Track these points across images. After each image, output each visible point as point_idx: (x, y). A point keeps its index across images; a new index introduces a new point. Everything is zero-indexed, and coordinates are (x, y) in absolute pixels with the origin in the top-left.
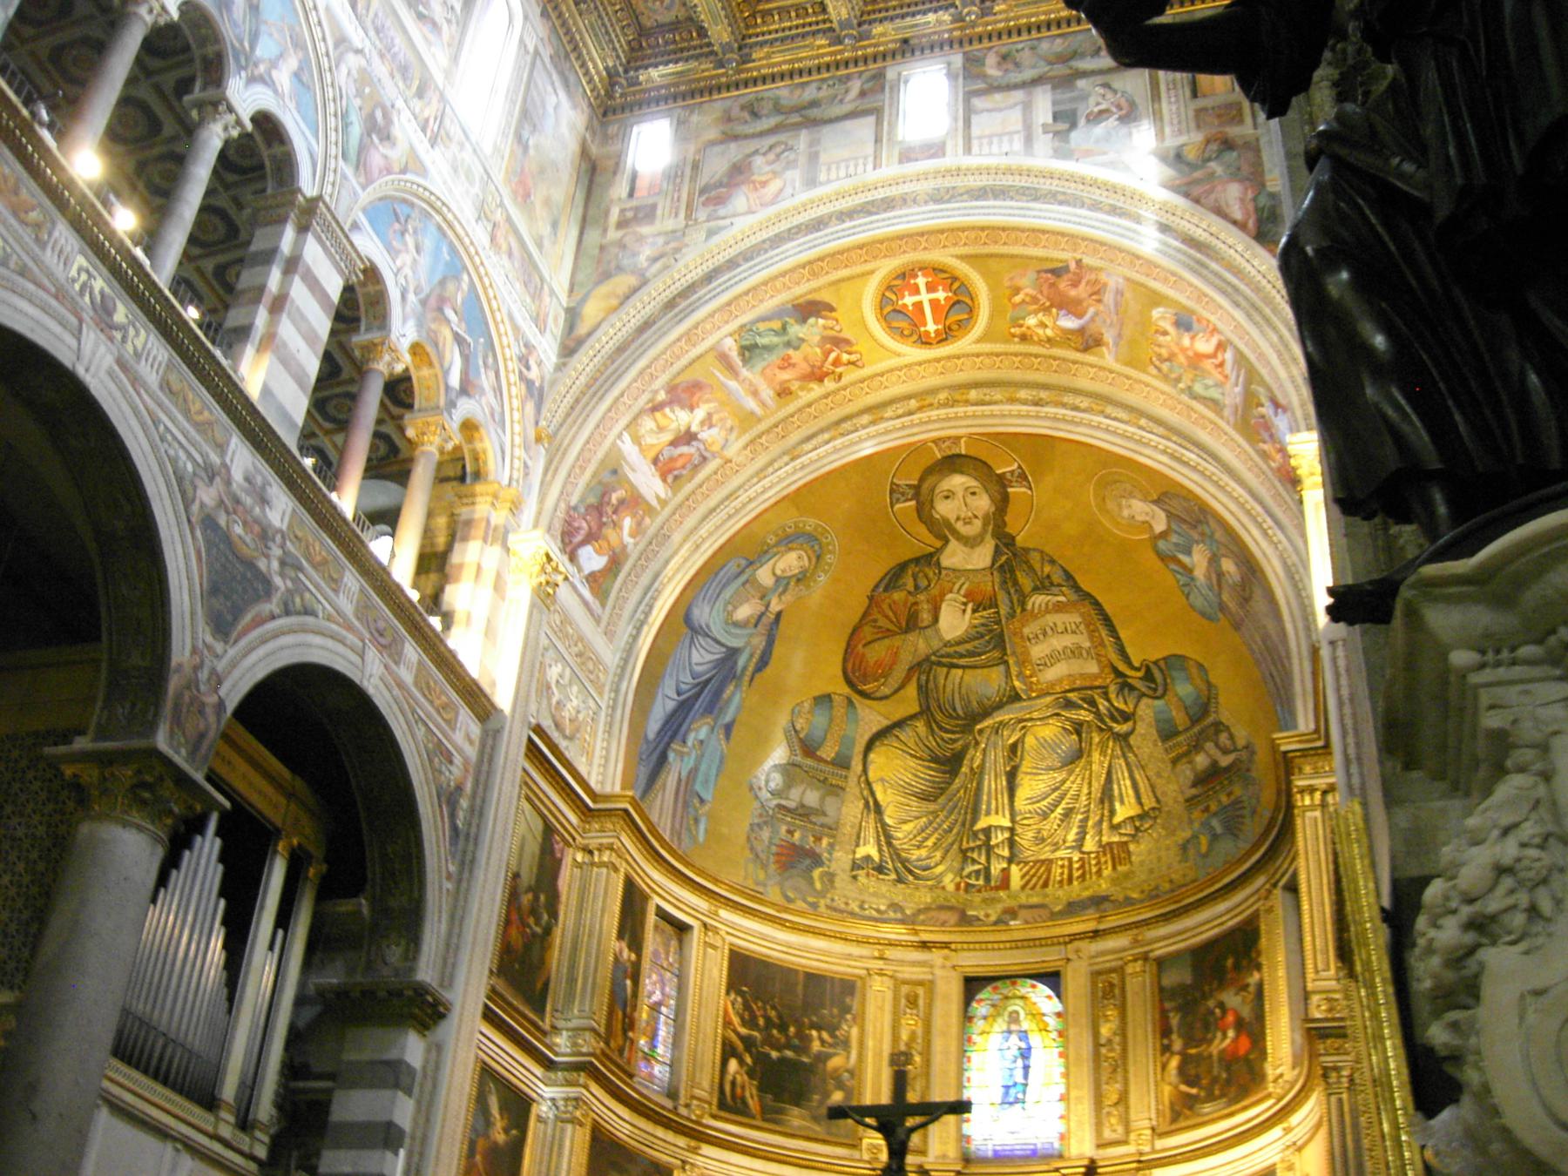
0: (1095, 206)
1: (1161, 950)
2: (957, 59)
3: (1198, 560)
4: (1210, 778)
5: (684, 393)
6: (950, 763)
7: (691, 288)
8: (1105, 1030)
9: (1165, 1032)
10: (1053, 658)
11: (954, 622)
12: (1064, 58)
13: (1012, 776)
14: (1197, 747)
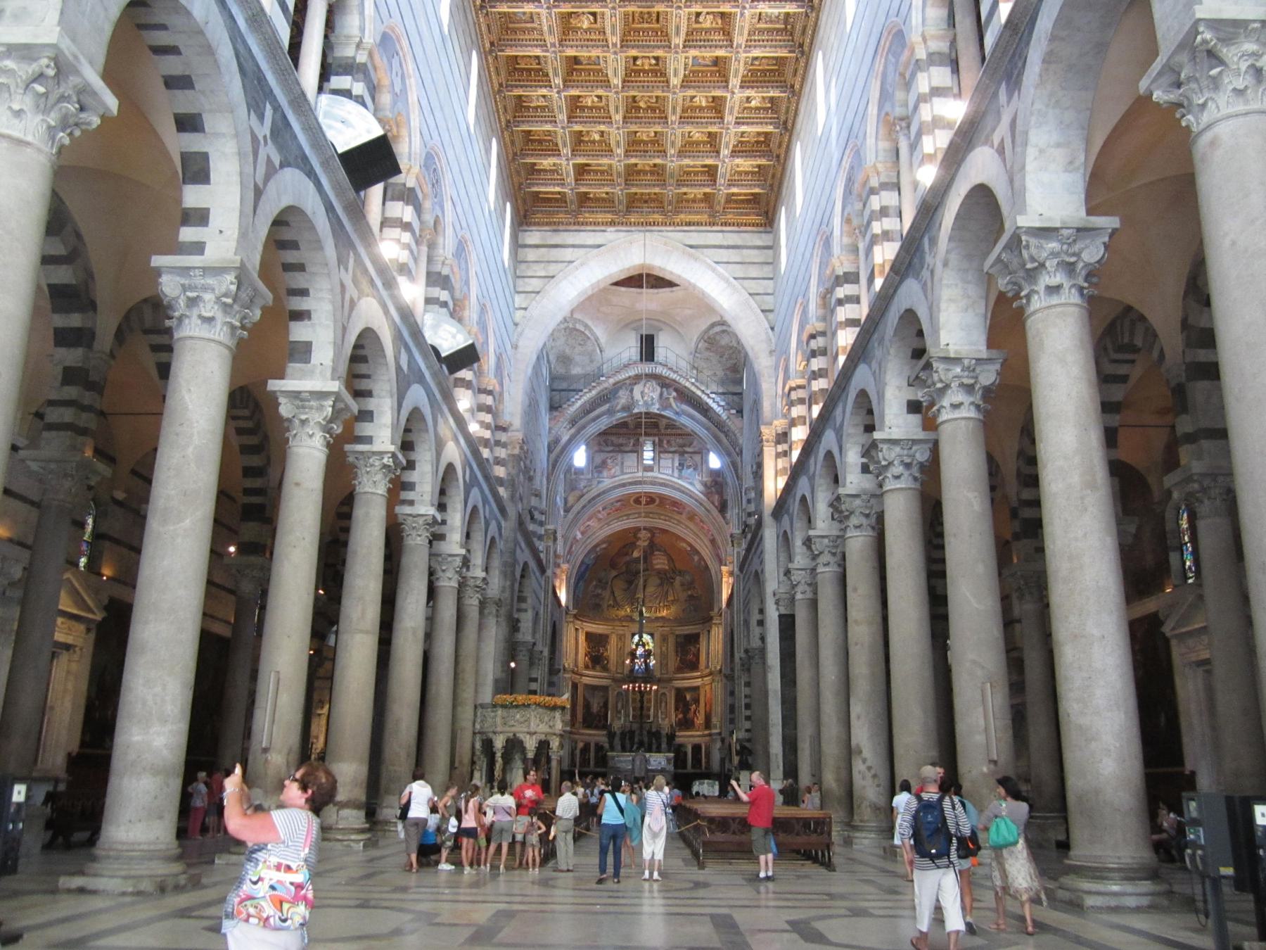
0: (687, 494)
1: (677, 633)
2: (657, 439)
3: (696, 558)
4: (691, 597)
5: (589, 519)
6: (630, 583)
7: (594, 498)
8: (664, 649)
9: (677, 652)
10: (658, 564)
11: (636, 554)
12: (683, 446)
13: (645, 587)
14: (689, 589)
